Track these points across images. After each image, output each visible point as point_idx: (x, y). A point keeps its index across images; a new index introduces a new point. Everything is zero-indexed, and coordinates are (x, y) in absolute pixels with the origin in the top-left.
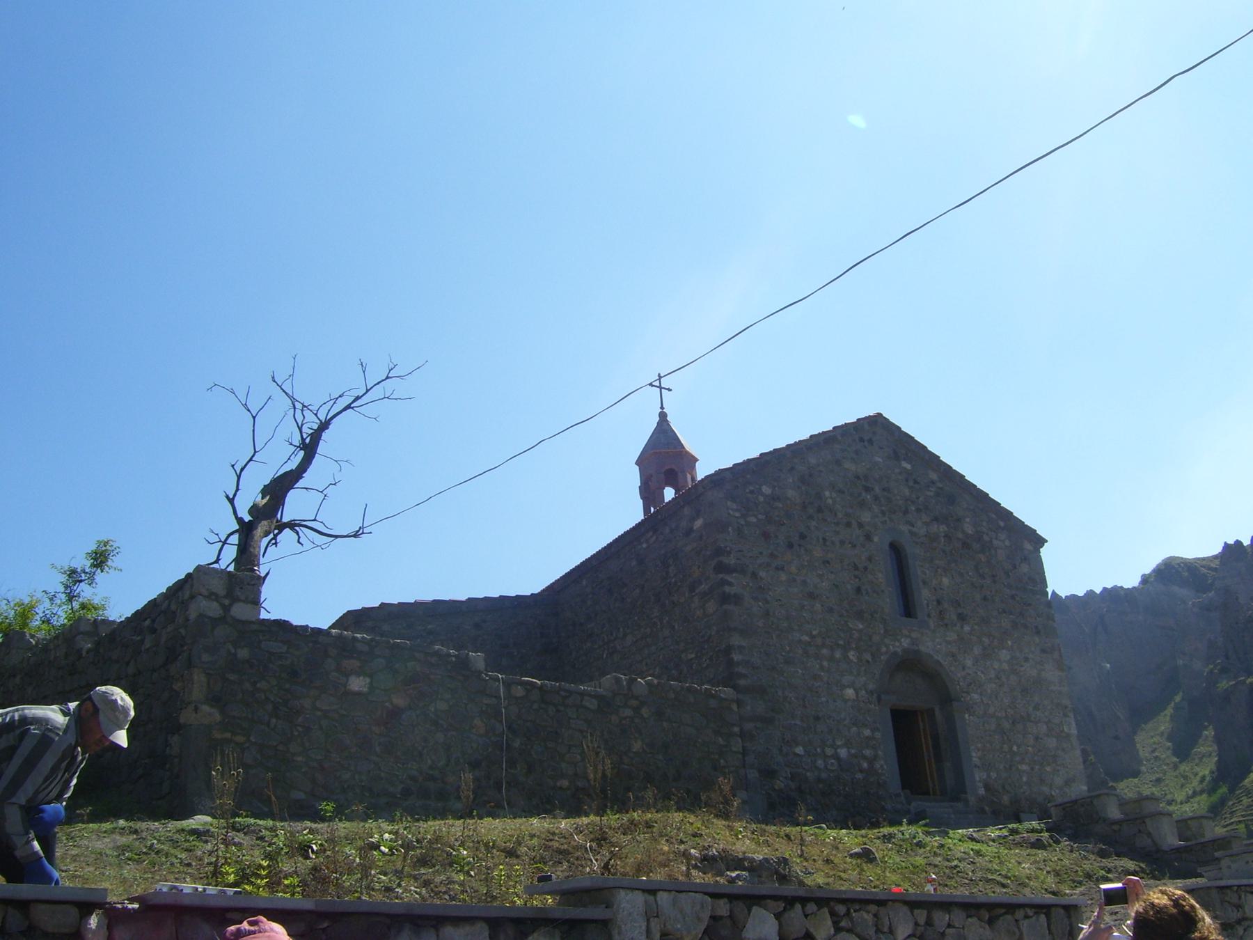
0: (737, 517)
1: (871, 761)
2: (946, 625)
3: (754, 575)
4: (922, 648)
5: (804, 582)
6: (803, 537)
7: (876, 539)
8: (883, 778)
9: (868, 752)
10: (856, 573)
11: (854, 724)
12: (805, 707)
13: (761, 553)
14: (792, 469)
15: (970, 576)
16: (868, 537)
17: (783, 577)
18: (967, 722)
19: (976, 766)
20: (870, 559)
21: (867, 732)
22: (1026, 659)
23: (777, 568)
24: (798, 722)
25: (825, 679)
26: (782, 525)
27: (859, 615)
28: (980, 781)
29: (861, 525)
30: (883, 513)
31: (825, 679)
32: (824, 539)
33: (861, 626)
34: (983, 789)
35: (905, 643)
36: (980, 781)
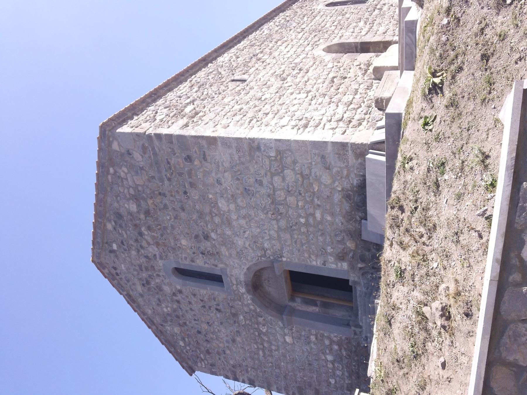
0: (205, 363)
1: (332, 342)
2: (217, 253)
3: (234, 366)
4: (242, 278)
5: (227, 342)
6: (199, 332)
7: (179, 287)
8: (343, 338)
9: (327, 342)
10: (207, 307)
11: (309, 343)
12: (304, 369)
13: (220, 359)
14: (162, 325)
15: (171, 218)
16: (180, 292)
17: (228, 352)
18: (288, 260)
19: (324, 264)
20: (195, 295)
21: (313, 338)
22: (219, 182)
23: (225, 353)
24: (315, 376)
25: (284, 351)
26: (198, 342)
27: (235, 315)
28: (337, 264)
29: (174, 294)
30: (158, 275)
31: (284, 351)
32: (195, 320)
33: (241, 317)
34: (343, 264)
35: (243, 290)
36: (337, 264)
